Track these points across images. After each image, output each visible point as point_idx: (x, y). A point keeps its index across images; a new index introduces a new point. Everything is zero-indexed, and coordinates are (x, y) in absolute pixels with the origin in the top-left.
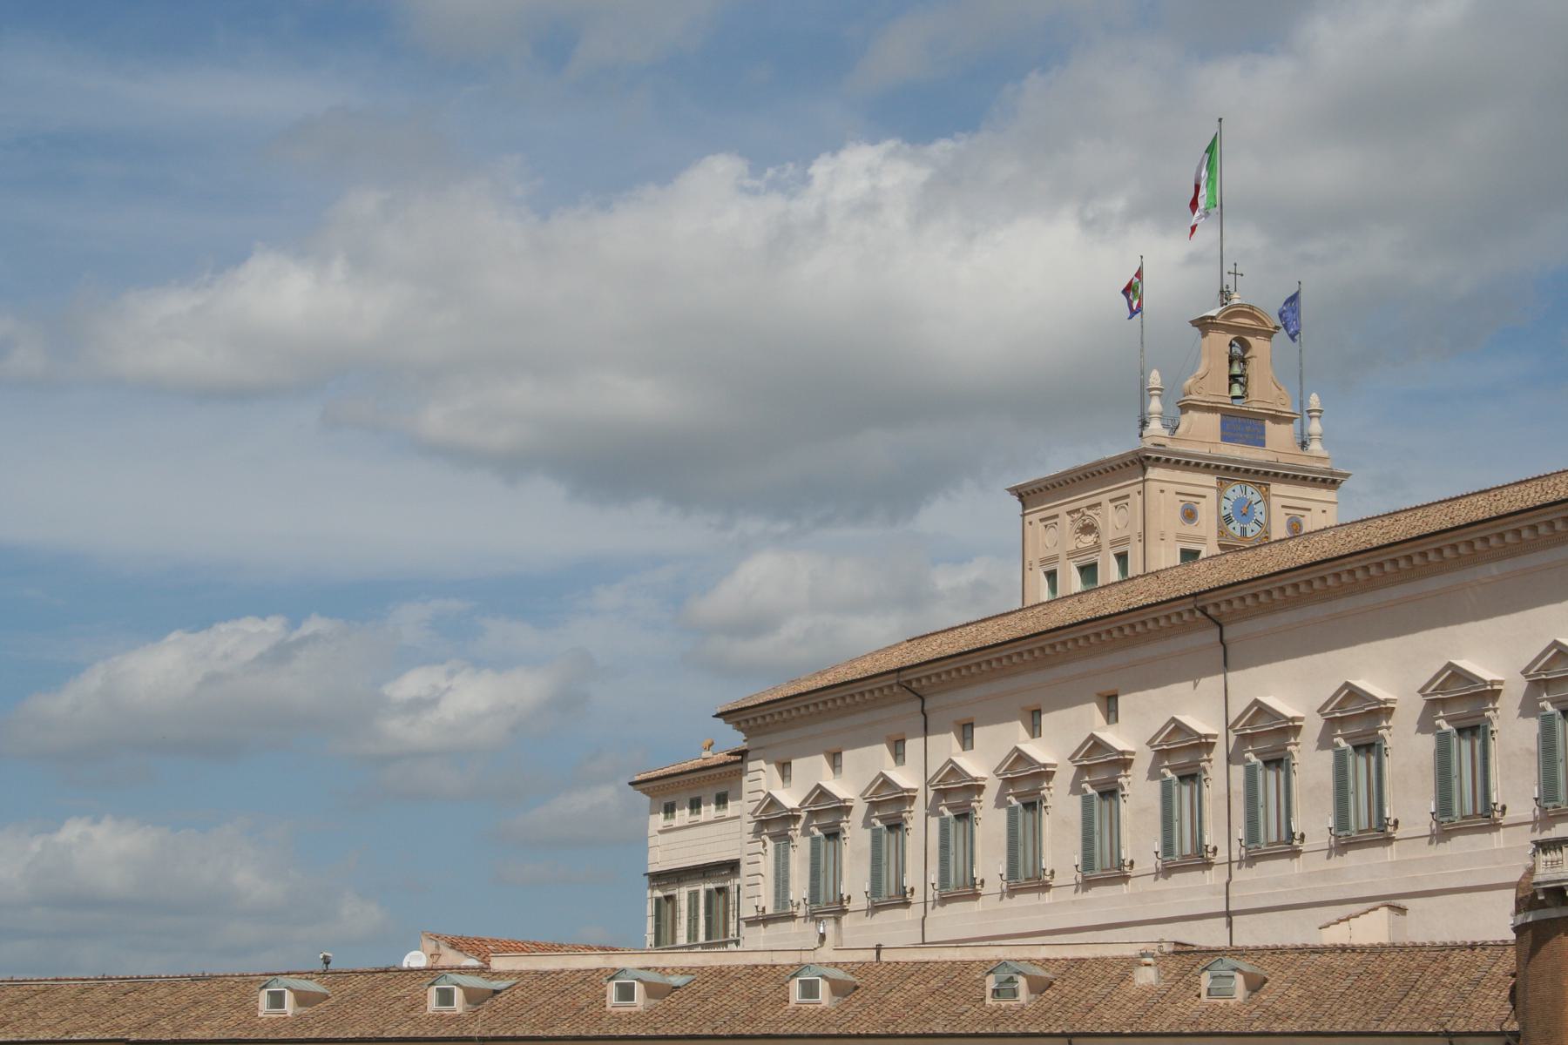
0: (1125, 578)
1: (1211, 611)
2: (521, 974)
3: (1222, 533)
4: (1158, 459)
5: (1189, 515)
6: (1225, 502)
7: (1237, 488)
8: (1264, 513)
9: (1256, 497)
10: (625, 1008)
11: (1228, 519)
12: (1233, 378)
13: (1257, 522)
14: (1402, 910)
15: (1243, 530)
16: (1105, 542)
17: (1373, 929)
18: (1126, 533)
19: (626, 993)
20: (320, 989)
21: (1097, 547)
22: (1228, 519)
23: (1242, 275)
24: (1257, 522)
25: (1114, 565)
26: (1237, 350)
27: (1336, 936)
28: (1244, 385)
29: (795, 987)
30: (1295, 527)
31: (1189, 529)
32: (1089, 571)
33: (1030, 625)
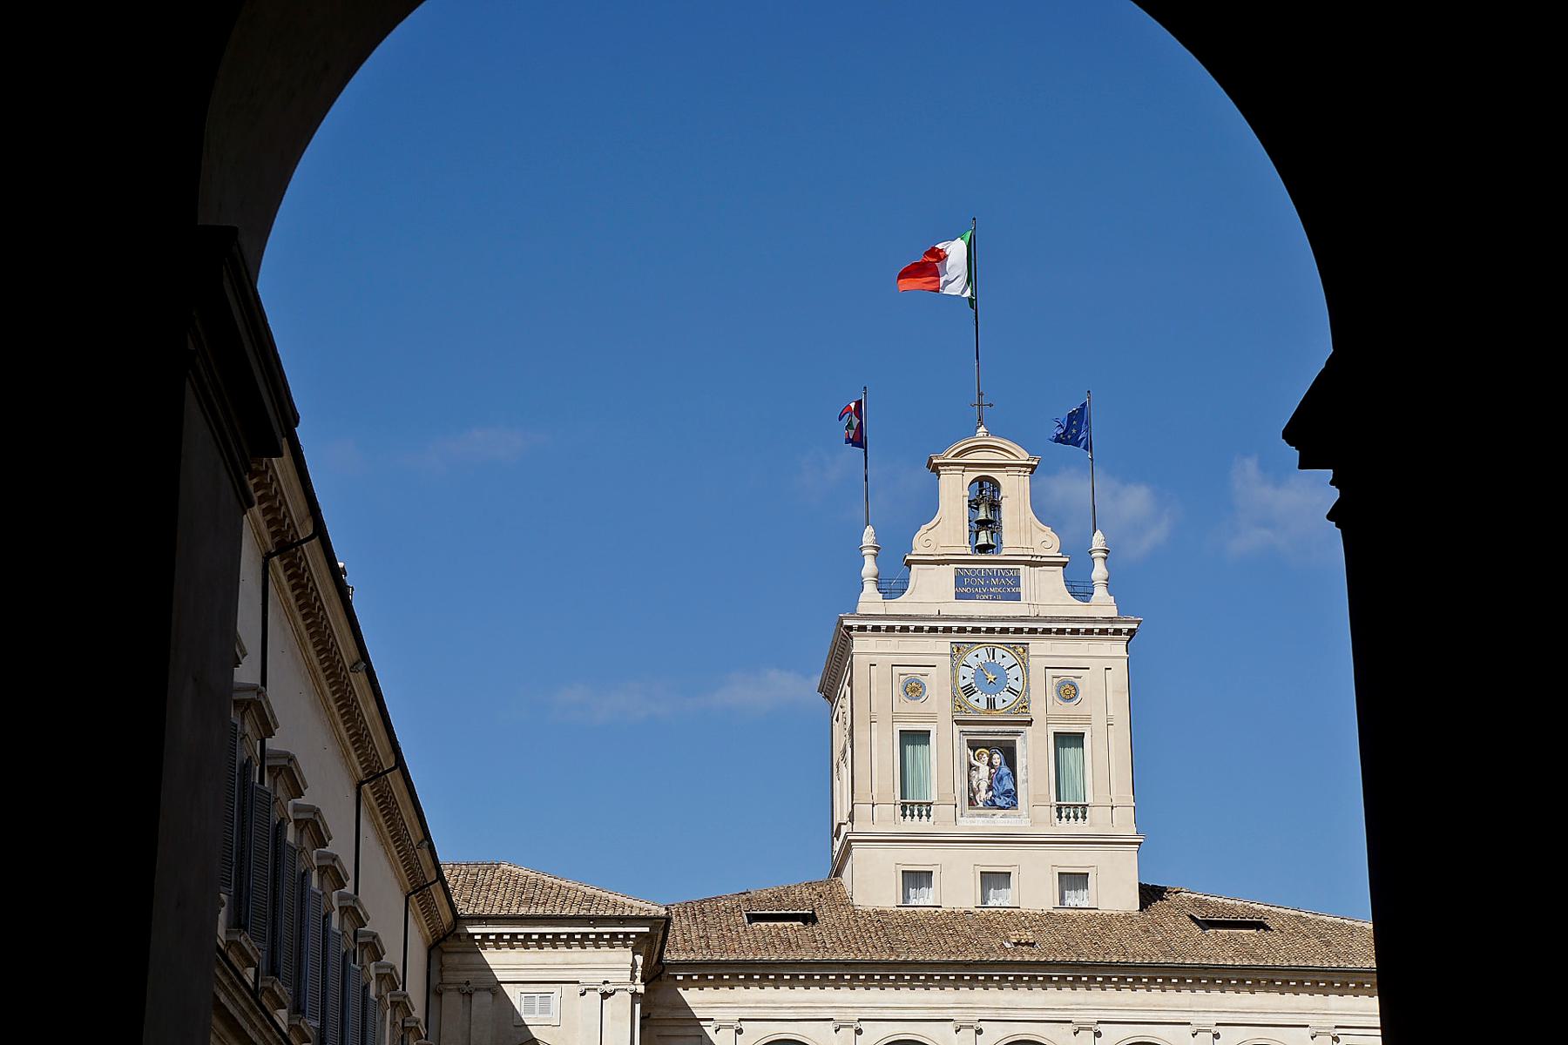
3: (958, 706)
4: (862, 628)
5: (914, 689)
6: (963, 671)
7: (982, 652)
8: (1021, 679)
9: (1010, 660)
11: (969, 691)
13: (1011, 690)
15: (991, 704)
22: (969, 691)
23: (991, 405)
24: (1011, 690)
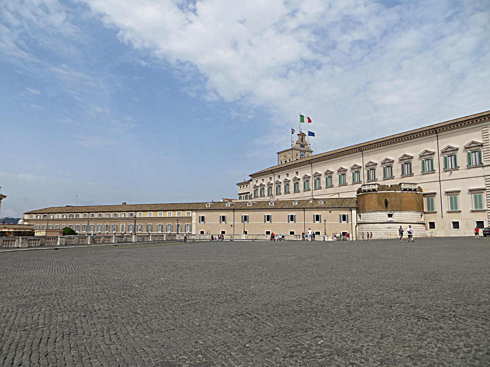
0: (282, 164)
1: (310, 162)
2: (235, 202)
3: (300, 157)
5: (297, 155)
10: (249, 206)
11: (301, 156)
12: (301, 141)
14: (339, 194)
16: (288, 158)
17: (336, 196)
18: (290, 157)
19: (249, 204)
20: (213, 204)
21: (287, 158)
22: (301, 156)
25: (289, 160)
26: (302, 137)
27: (332, 197)
28: (302, 142)
29: (270, 203)
30: (308, 156)
31: (297, 157)
32: (286, 161)
33: (278, 167)
